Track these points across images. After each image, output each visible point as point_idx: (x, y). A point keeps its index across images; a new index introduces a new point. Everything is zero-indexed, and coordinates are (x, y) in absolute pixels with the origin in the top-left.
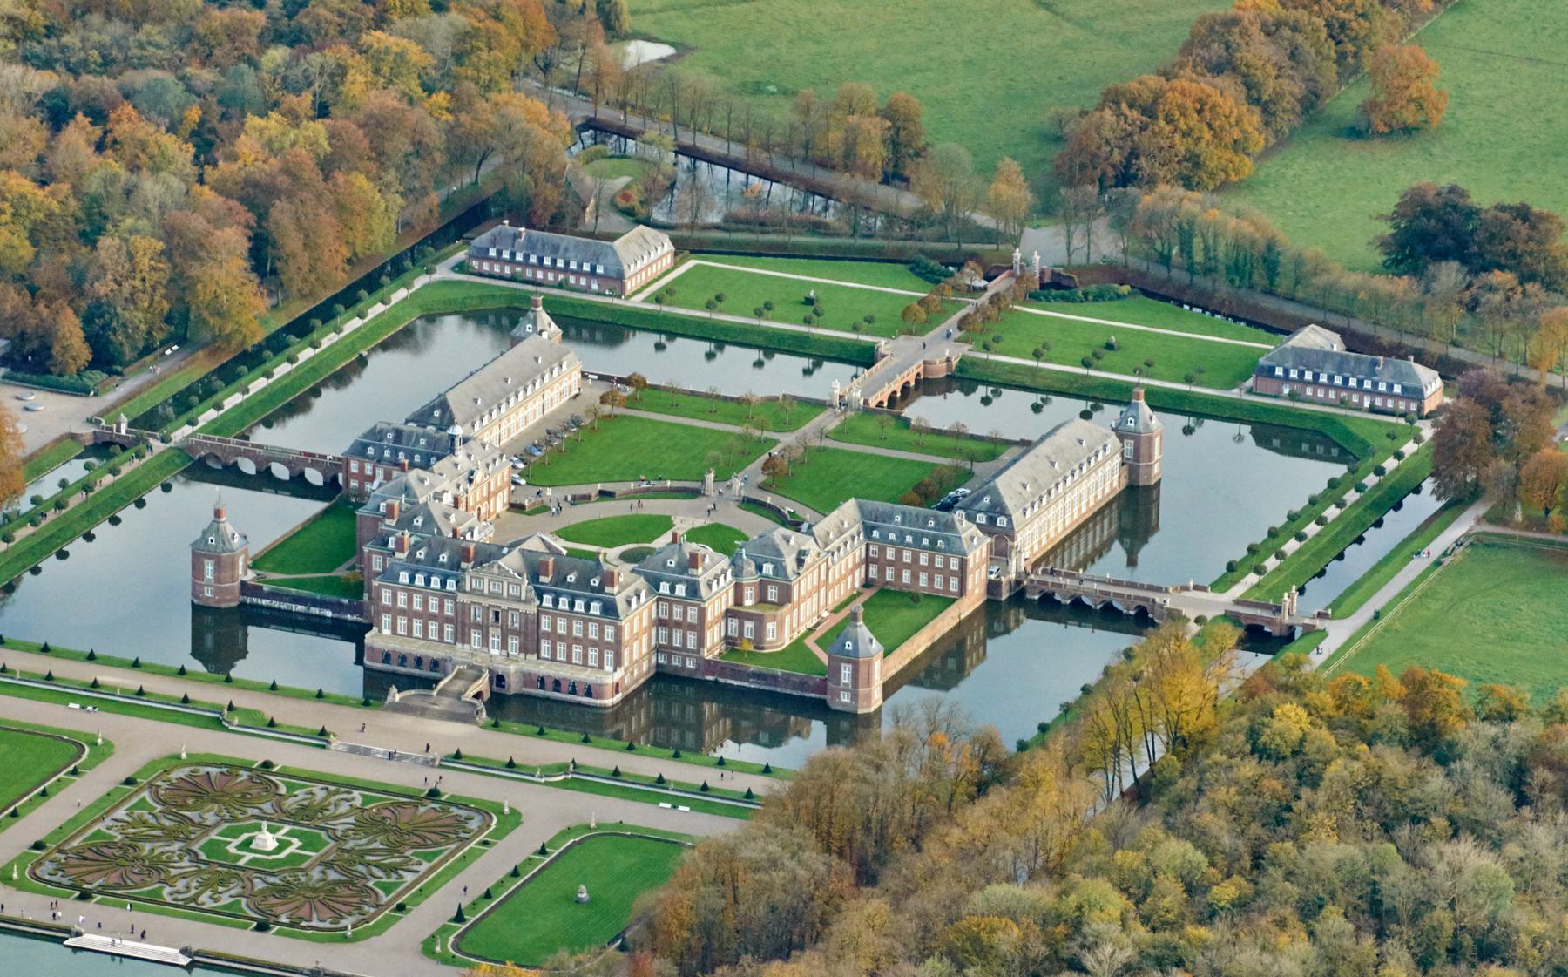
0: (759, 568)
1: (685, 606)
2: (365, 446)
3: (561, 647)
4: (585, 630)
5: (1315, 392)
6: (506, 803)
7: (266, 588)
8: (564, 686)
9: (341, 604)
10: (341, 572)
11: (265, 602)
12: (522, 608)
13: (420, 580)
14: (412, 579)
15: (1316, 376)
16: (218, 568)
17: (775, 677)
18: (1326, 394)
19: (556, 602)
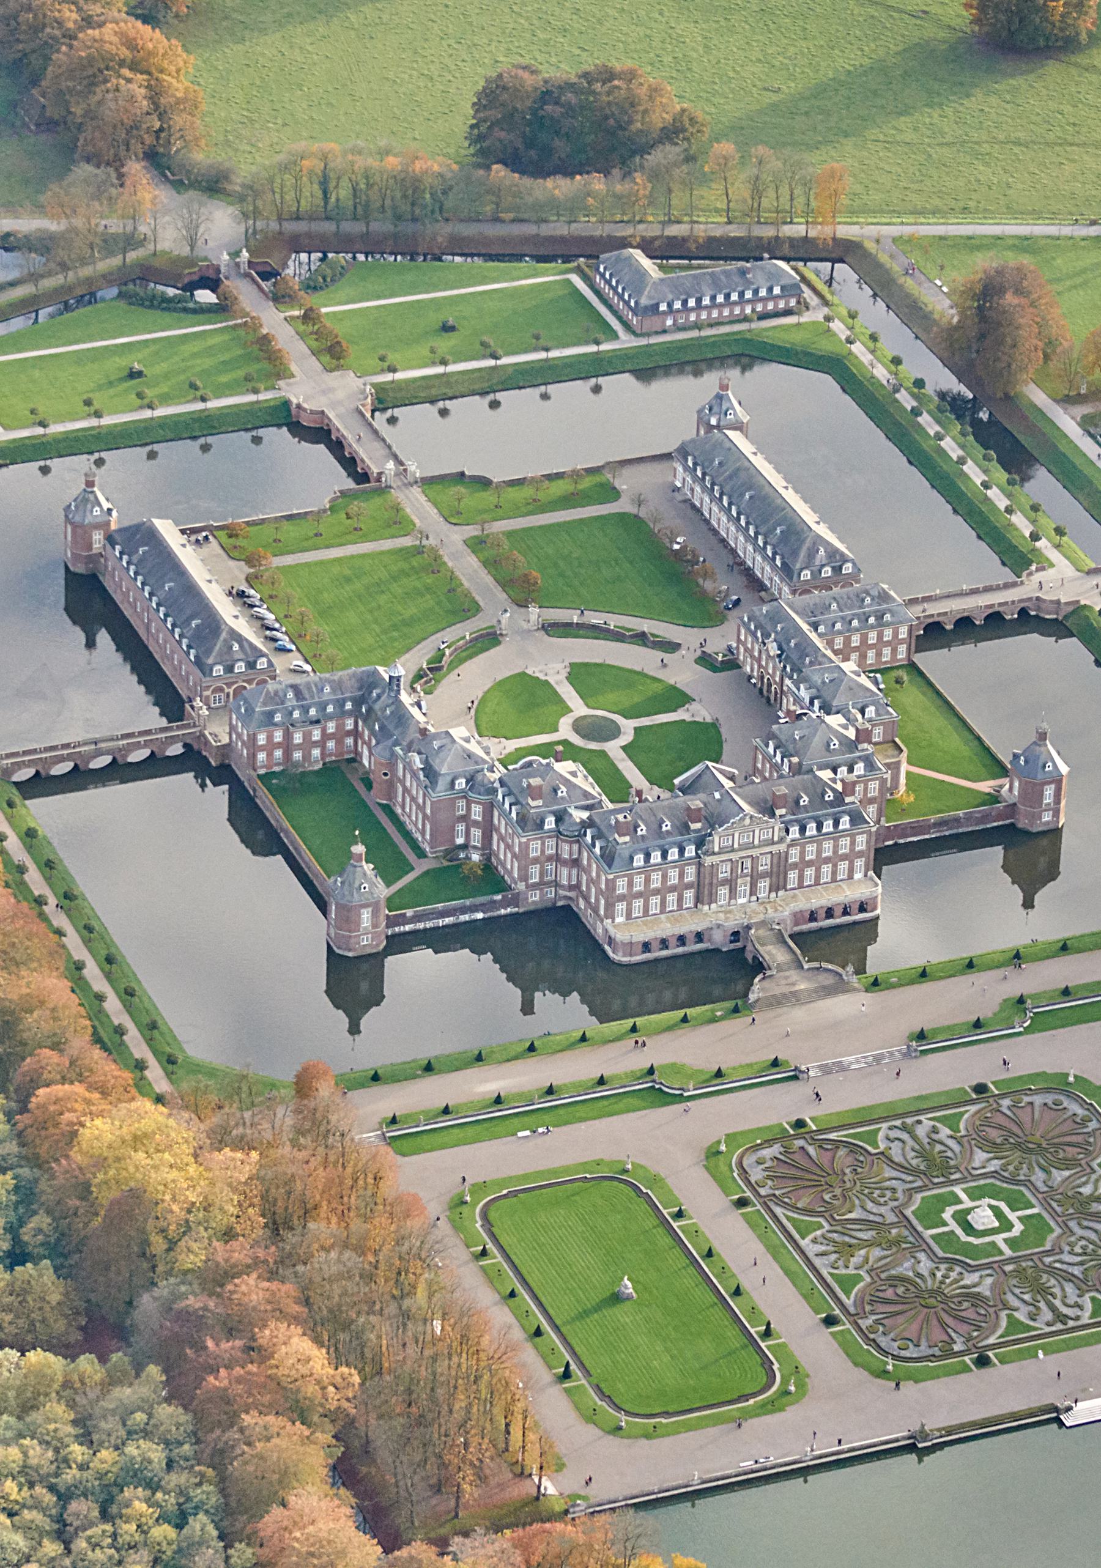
0: (863, 712)
1: (866, 783)
2: (270, 715)
3: (810, 872)
4: (836, 848)
5: (698, 316)
6: (1072, 1072)
7: (409, 913)
8: (838, 911)
9: (495, 902)
10: (421, 867)
11: (408, 928)
12: (774, 849)
13: (656, 857)
14: (648, 856)
15: (699, 301)
16: (375, 914)
17: (957, 820)
18: (709, 314)
19: (803, 830)
